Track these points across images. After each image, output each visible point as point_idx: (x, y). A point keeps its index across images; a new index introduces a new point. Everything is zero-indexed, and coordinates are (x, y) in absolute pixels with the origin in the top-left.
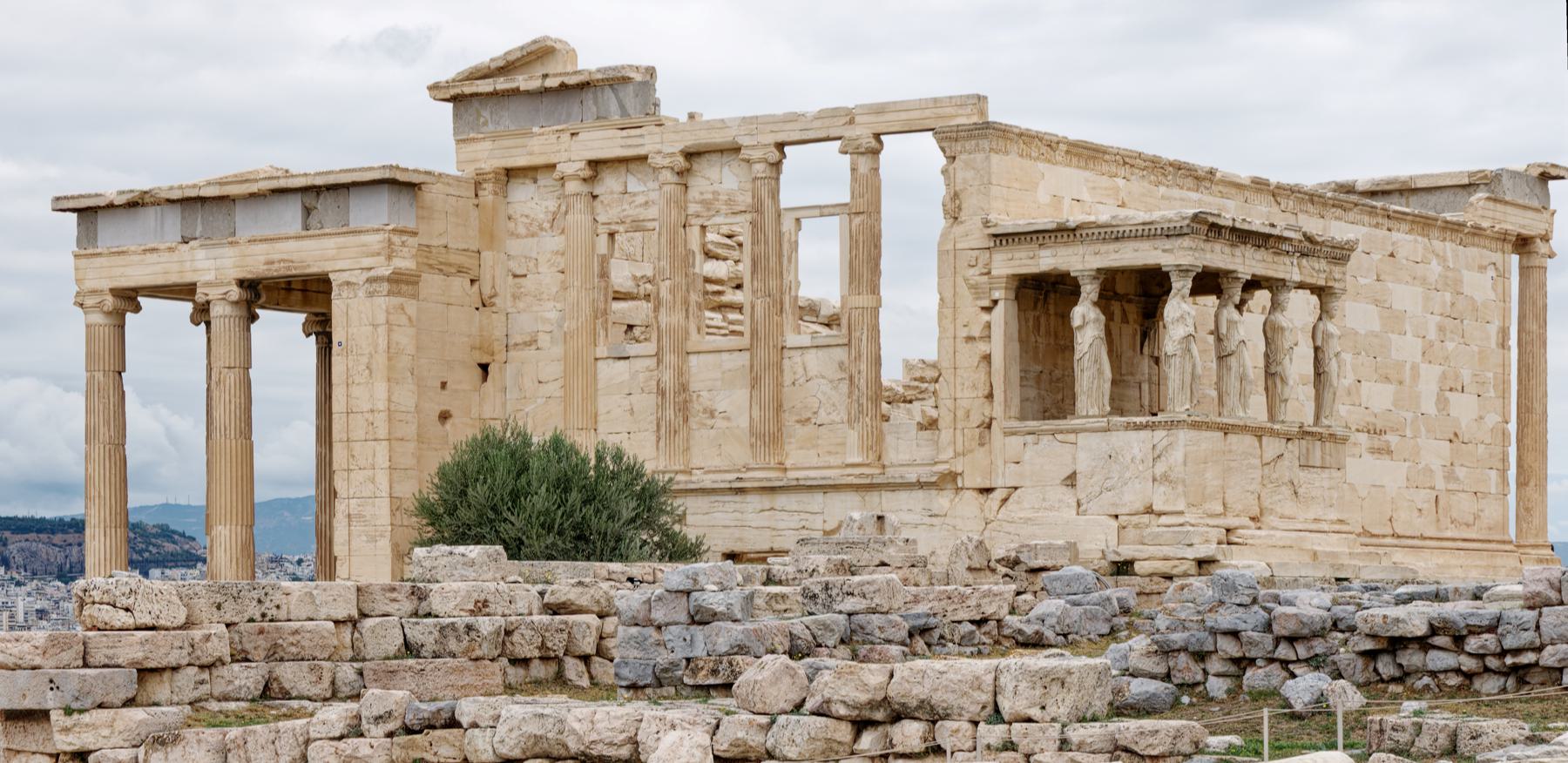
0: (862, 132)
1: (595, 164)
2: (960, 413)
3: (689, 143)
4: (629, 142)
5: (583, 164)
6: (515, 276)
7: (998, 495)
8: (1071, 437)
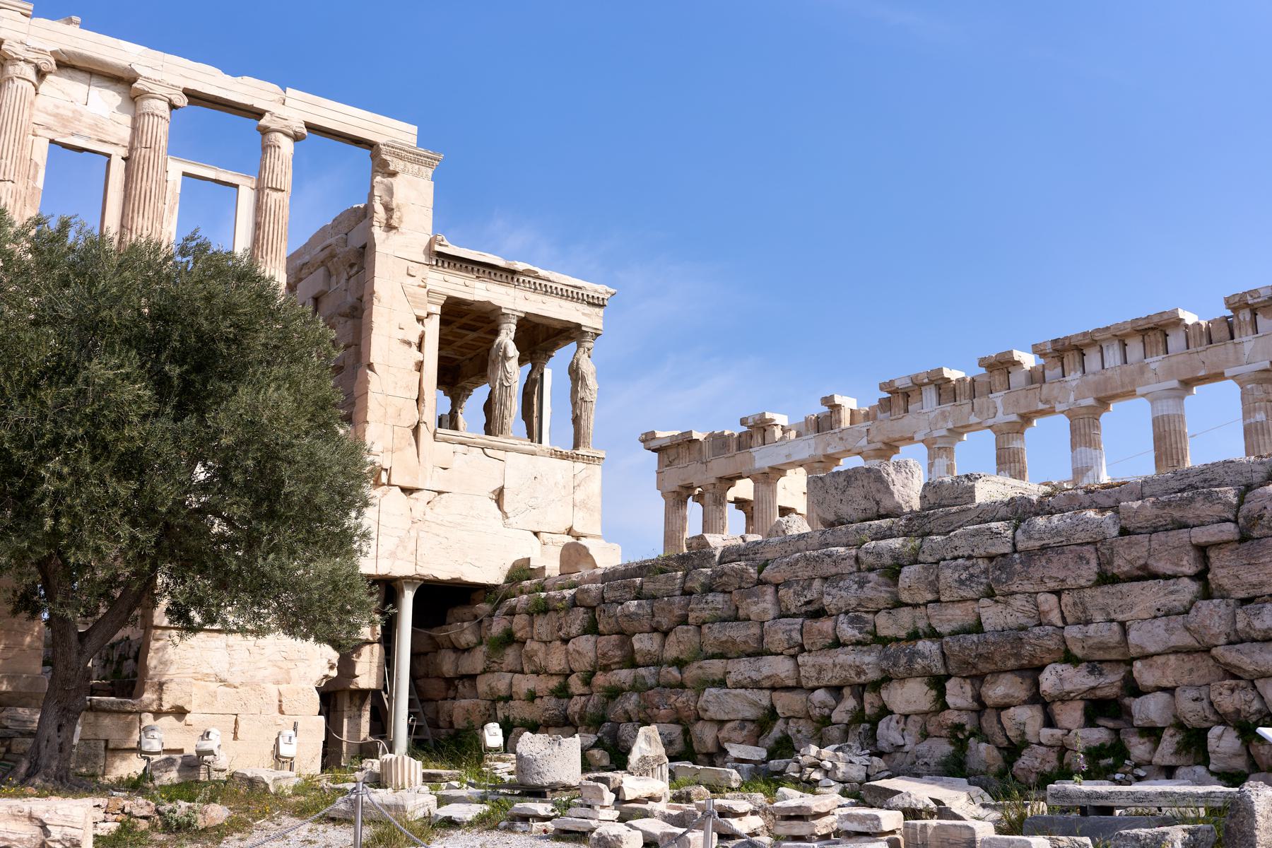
2: (391, 411)
3: (65, 48)
7: (423, 496)
8: (500, 454)
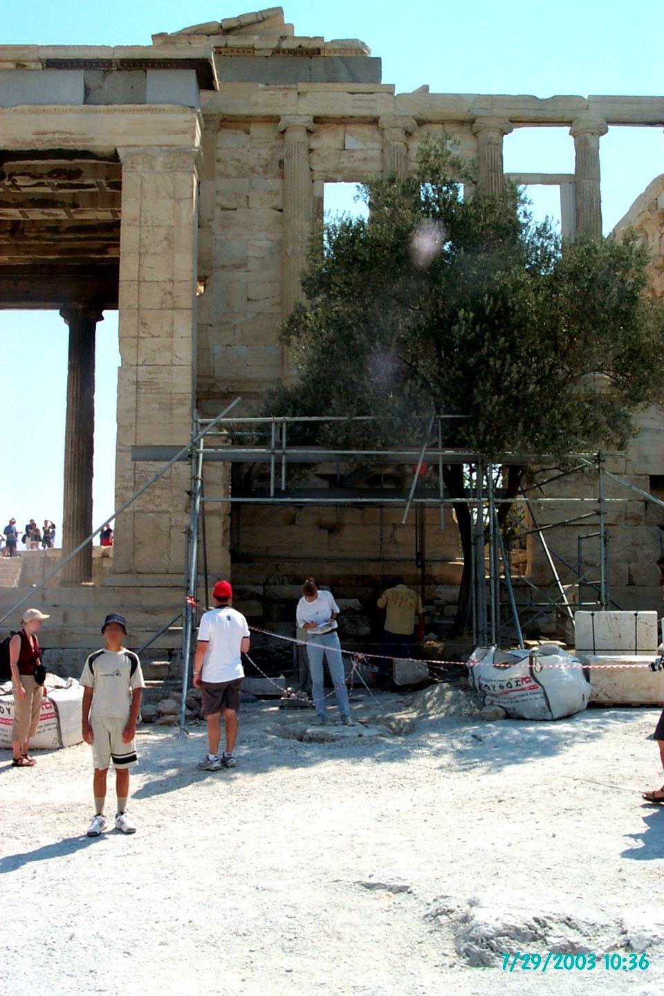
0: (594, 116)
1: (317, 120)
4: (359, 103)
5: (311, 119)
6: (223, 209)
